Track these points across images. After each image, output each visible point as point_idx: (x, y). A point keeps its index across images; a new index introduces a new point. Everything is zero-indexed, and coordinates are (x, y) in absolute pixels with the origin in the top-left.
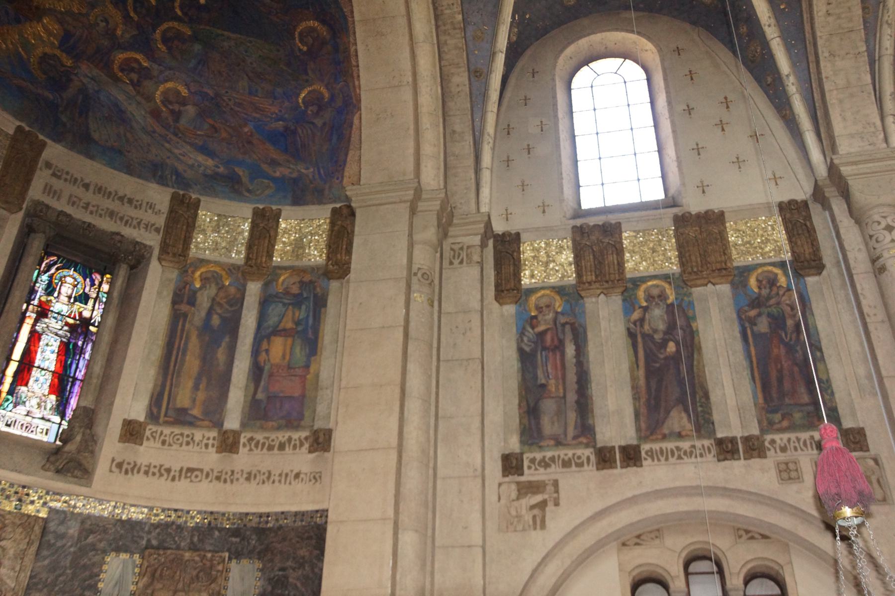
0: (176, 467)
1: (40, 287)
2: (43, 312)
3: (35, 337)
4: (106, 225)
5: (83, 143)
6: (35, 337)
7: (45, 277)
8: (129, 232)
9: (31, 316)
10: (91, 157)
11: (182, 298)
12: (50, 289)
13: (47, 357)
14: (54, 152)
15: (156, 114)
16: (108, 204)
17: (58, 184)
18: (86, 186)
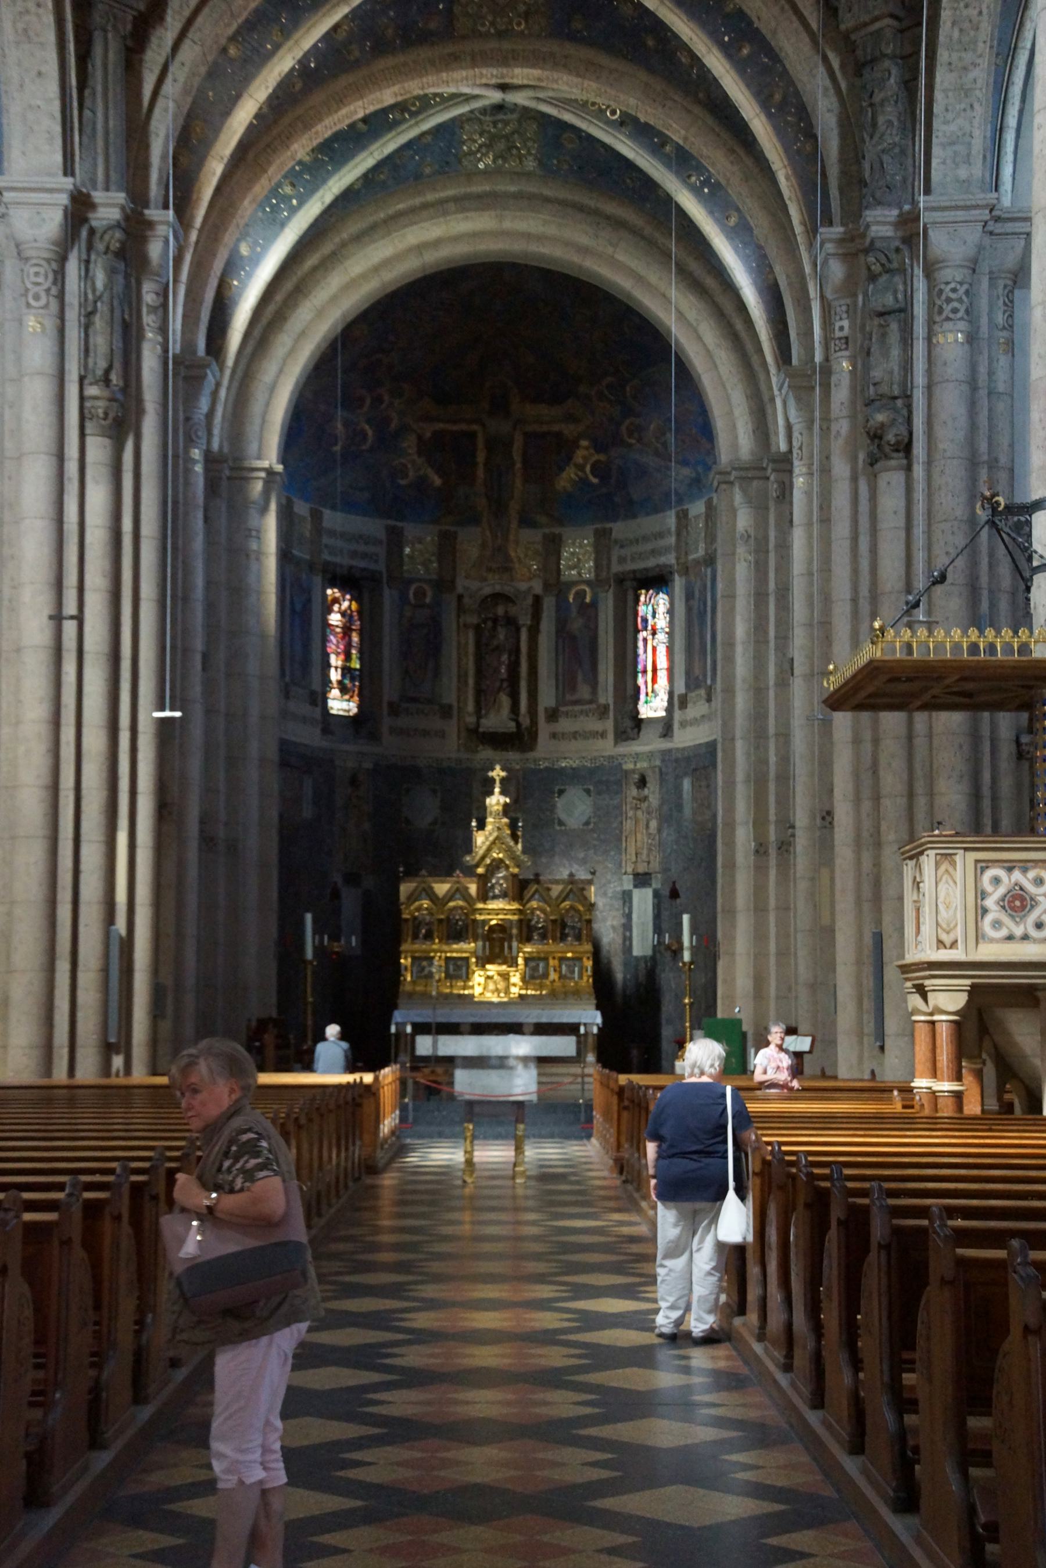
0: (698, 716)
1: (650, 617)
2: (654, 633)
3: (654, 649)
4: (651, 563)
5: (631, 510)
6: (654, 649)
7: (650, 608)
8: (663, 560)
9: (650, 637)
10: (634, 516)
11: (689, 596)
12: (654, 617)
13: (662, 662)
14: (619, 529)
15: (657, 453)
16: (649, 546)
17: (623, 552)
18: (637, 541)
